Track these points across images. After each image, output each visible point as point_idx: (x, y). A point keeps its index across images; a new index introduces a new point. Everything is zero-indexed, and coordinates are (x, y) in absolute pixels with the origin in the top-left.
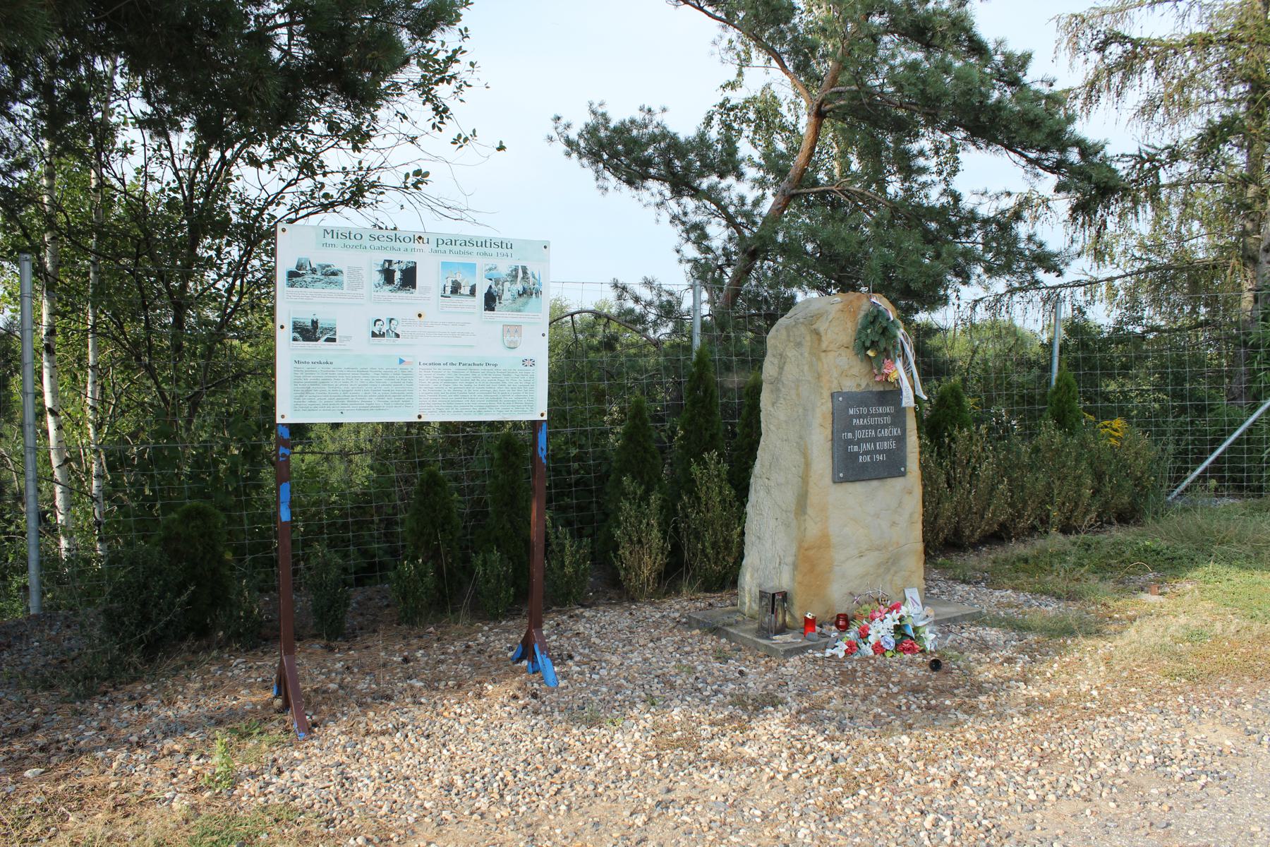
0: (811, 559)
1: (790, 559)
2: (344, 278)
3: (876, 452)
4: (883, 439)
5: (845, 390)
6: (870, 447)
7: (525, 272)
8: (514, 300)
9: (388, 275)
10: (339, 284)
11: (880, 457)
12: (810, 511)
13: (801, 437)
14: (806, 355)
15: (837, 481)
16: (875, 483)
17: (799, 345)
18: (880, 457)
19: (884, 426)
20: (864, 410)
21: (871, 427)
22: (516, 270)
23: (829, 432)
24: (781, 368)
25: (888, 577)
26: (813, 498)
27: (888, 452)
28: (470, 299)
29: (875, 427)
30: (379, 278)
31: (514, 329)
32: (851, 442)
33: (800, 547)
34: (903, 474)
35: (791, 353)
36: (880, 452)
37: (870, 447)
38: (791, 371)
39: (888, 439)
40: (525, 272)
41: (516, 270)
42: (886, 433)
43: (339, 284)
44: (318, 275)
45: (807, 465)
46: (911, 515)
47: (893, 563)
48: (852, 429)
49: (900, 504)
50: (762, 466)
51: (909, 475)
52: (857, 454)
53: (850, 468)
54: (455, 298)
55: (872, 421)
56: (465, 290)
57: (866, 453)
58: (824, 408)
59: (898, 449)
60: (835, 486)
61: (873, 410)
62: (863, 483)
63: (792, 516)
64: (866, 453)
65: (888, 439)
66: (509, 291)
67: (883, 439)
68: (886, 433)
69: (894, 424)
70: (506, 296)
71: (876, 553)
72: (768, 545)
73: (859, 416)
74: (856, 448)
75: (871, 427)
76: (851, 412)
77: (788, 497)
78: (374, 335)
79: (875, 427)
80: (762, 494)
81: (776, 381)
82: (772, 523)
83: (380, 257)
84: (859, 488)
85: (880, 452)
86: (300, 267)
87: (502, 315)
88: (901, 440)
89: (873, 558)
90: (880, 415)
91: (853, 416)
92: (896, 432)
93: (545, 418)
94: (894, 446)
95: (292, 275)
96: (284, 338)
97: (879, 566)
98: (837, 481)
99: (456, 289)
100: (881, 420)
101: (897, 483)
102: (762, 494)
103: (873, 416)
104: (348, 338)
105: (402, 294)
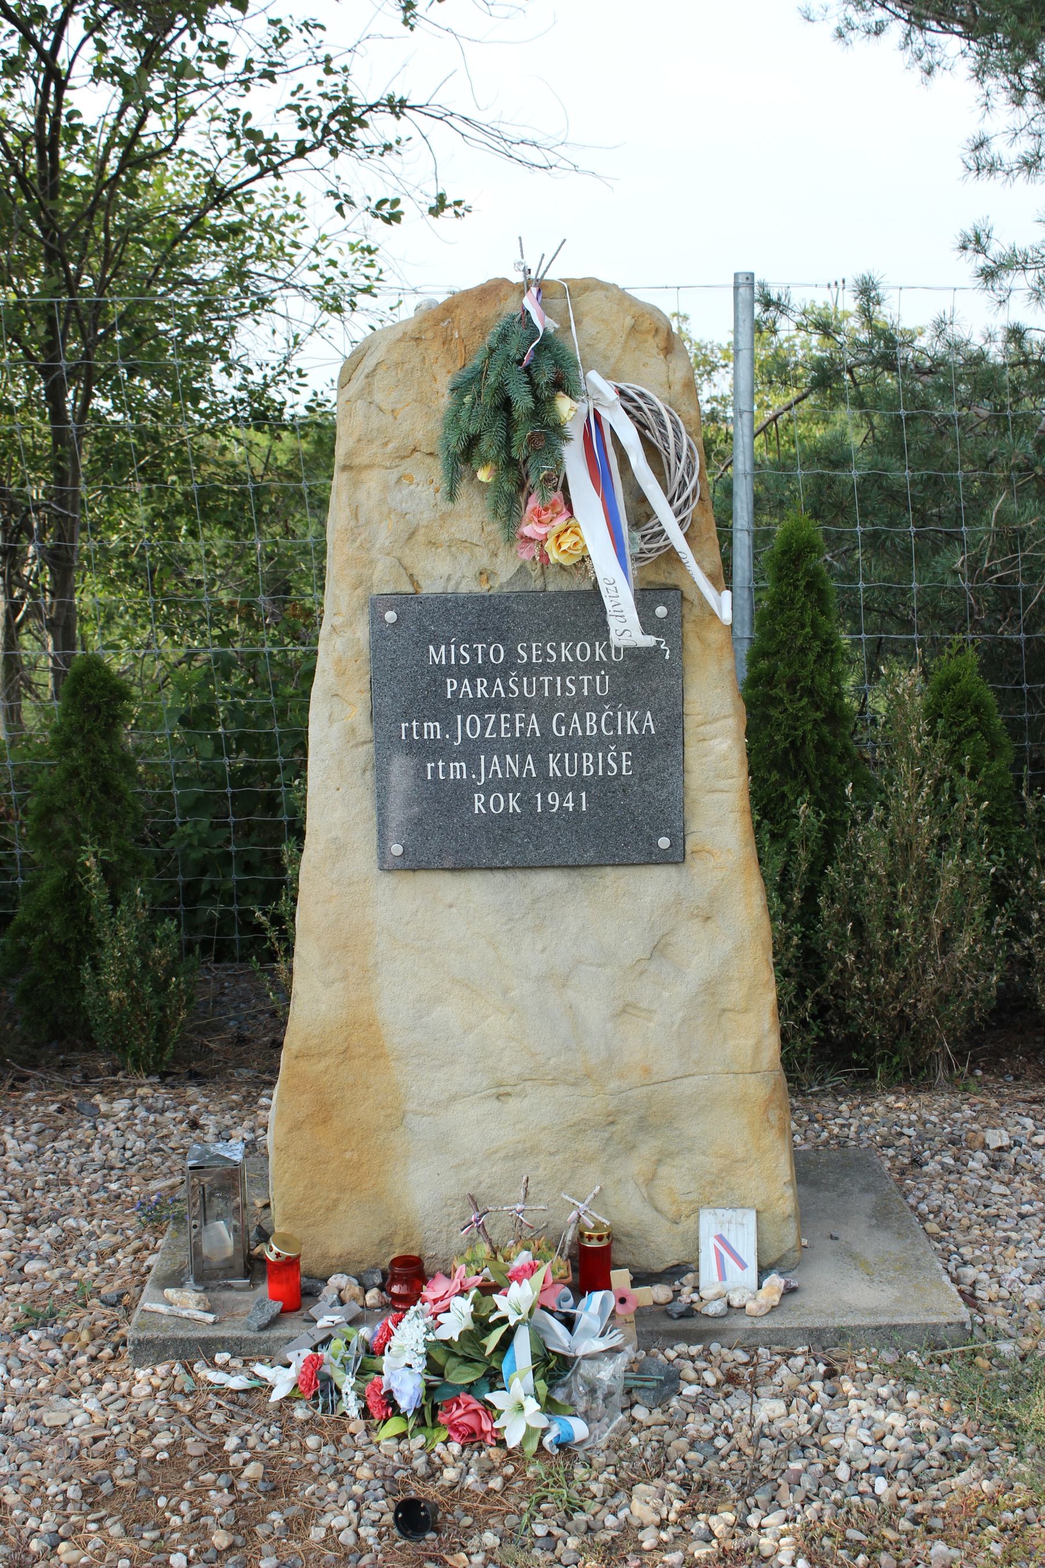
3: (546, 782)
4: (575, 745)
5: (430, 587)
16: (546, 881)
19: (581, 704)
25: (636, 1166)
27: (602, 788)
34: (676, 857)
36: (562, 785)
39: (599, 744)
42: (591, 724)
46: (710, 987)
47: (643, 1125)
48: (445, 711)
49: (659, 949)
51: (696, 866)
52: (463, 791)
55: (524, 688)
59: (644, 778)
60: (389, 881)
61: (528, 653)
62: (499, 877)
65: (599, 744)
68: (591, 724)
69: (624, 697)
71: (561, 1091)
73: (473, 672)
74: (458, 770)
76: (437, 655)
79: (545, 708)
85: (562, 785)
89: (538, 1110)
90: (562, 669)
91: (446, 671)
97: (579, 1128)
103: (529, 669)
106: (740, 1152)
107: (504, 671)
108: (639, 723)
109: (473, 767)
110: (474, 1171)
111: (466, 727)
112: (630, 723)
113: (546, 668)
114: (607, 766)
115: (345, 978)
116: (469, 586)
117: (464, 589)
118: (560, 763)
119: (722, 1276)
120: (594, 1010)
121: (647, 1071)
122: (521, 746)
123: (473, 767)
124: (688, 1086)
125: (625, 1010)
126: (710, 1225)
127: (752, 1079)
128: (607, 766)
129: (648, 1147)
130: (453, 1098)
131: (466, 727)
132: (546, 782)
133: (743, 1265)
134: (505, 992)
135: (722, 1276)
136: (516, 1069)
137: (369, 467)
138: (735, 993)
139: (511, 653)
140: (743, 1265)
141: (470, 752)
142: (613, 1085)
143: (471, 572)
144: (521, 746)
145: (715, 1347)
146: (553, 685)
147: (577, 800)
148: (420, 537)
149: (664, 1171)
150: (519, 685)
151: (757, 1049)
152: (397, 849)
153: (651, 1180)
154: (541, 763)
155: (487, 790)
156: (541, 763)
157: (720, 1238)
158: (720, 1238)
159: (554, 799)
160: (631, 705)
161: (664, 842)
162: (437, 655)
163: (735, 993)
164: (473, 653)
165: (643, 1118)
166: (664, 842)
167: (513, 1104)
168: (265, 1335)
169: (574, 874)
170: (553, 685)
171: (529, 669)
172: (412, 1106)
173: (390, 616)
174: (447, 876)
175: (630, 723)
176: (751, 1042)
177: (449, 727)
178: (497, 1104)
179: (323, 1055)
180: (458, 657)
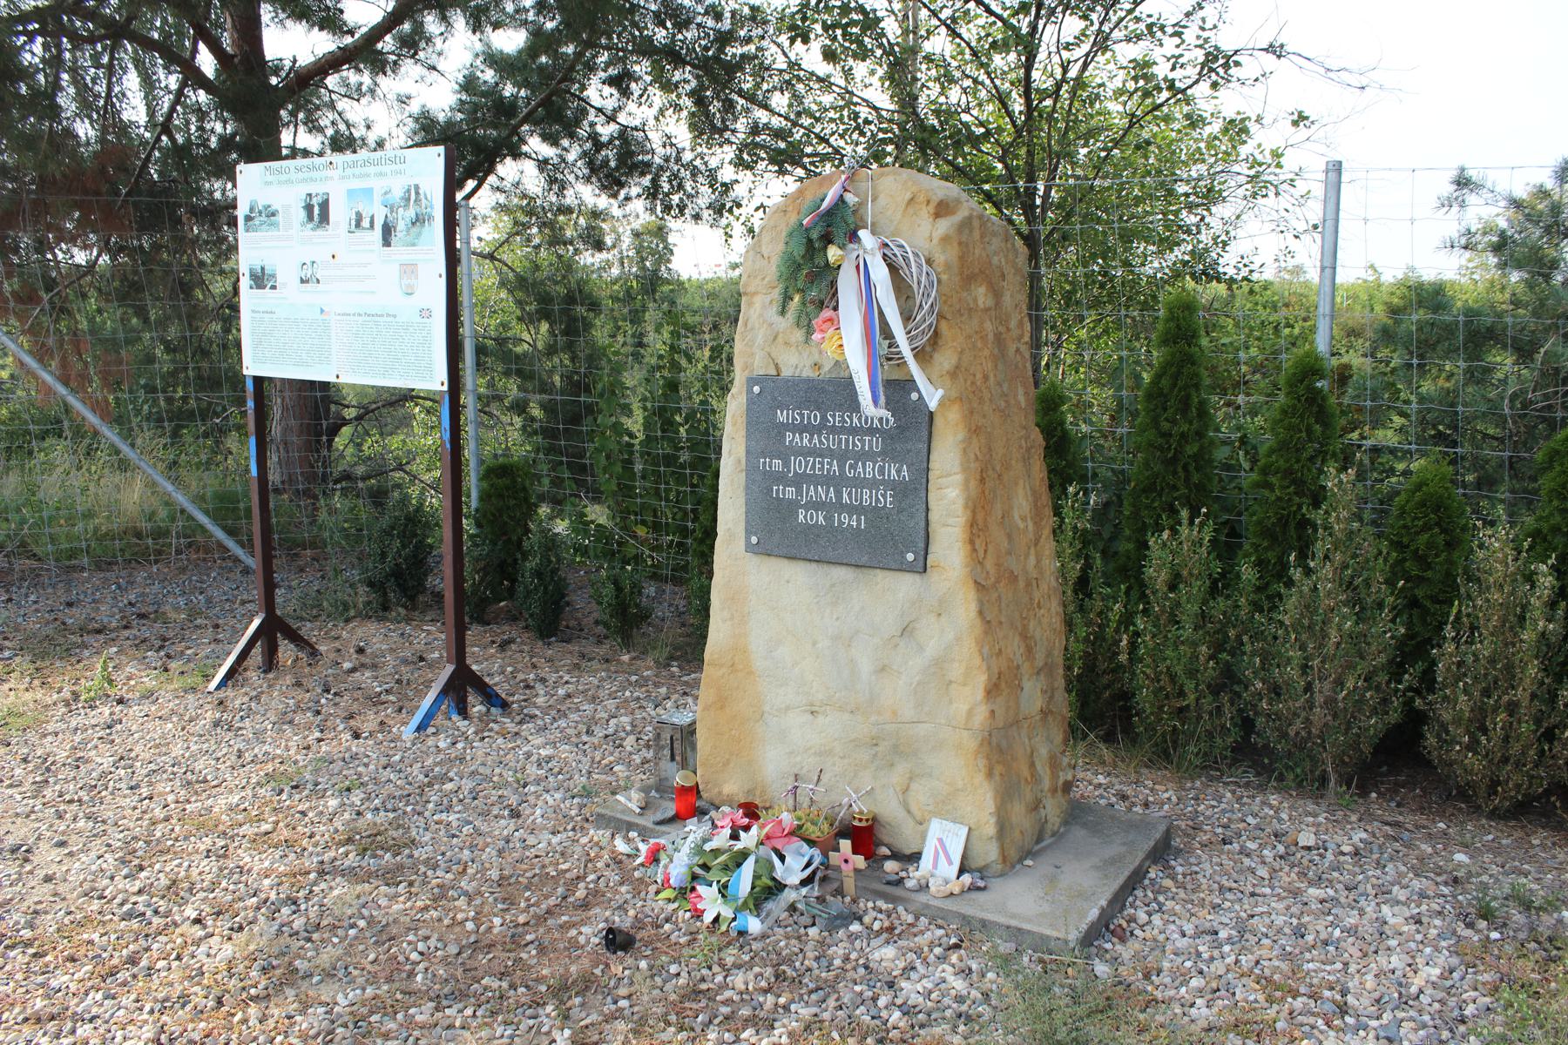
2: (279, 218)
3: (841, 507)
4: (859, 483)
5: (786, 372)
7: (417, 193)
8: (408, 230)
9: (309, 208)
10: (275, 225)
11: (849, 521)
19: (864, 456)
20: (815, 418)
21: (830, 453)
22: (409, 191)
25: (897, 776)
27: (874, 513)
28: (369, 233)
29: (842, 457)
30: (303, 214)
31: (409, 269)
32: (780, 478)
36: (851, 510)
39: (873, 484)
40: (417, 193)
41: (409, 191)
42: (869, 470)
43: (275, 225)
44: (263, 218)
46: (939, 664)
49: (906, 631)
51: (933, 575)
52: (793, 506)
54: (359, 234)
56: (366, 223)
57: (817, 506)
64: (817, 506)
65: (873, 484)
66: (404, 217)
67: (859, 483)
68: (869, 470)
70: (401, 226)
73: (802, 429)
75: (830, 453)
76: (782, 417)
78: (302, 281)
79: (842, 457)
83: (301, 191)
86: (252, 210)
87: (399, 252)
93: (445, 388)
94: (887, 500)
95: (248, 219)
96: (245, 283)
99: (358, 225)
100: (856, 443)
101: (904, 586)
103: (834, 430)
104: (284, 284)
105: (320, 232)
106: (960, 784)
107: (818, 430)
108: (899, 472)
109: (799, 492)
110: (798, 759)
111: (797, 465)
112: (893, 472)
113: (843, 430)
114: (878, 500)
115: (732, 619)
116: (808, 373)
117: (804, 375)
118: (850, 494)
119: (935, 866)
120: (866, 666)
121: (895, 713)
122: (826, 480)
123: (799, 492)
124: (922, 729)
125: (882, 669)
126: (936, 828)
127: (965, 733)
128: (878, 500)
129: (902, 769)
130: (788, 708)
132: (841, 507)
133: (950, 863)
134: (814, 644)
135: (935, 866)
136: (820, 696)
137: (755, 293)
138: (956, 671)
139: (824, 418)
140: (950, 863)
141: (799, 481)
142: (873, 718)
143: (809, 363)
144: (826, 480)
145: (900, 909)
146: (847, 441)
147: (859, 521)
148: (780, 339)
150: (827, 439)
151: (970, 713)
152: (754, 540)
153: (906, 790)
154: (839, 494)
155: (807, 507)
156: (839, 494)
157: (940, 840)
158: (940, 840)
159: (845, 518)
160: (894, 460)
161: (910, 557)
162: (782, 417)
163: (956, 671)
164: (802, 415)
165: (895, 746)
166: (910, 557)
167: (820, 719)
168: (658, 828)
169: (858, 570)
170: (847, 441)
171: (834, 430)
172: (767, 708)
173: (756, 389)
174: (786, 561)
175: (893, 472)
176: (966, 707)
177: (786, 464)
178: (810, 717)
179: (722, 666)
180: (794, 419)
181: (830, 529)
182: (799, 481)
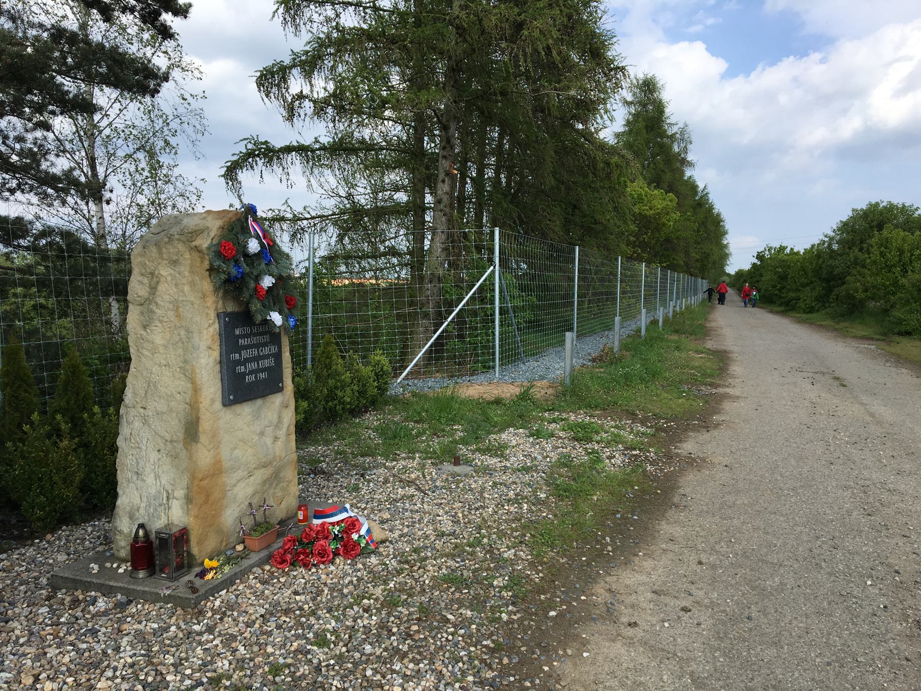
0: (203, 490)
1: (180, 493)
6: (253, 366)
11: (262, 376)
12: (203, 439)
13: (185, 362)
14: (187, 274)
15: (227, 403)
16: (259, 402)
17: (174, 263)
18: (262, 376)
23: (216, 354)
24: (153, 289)
25: (271, 491)
26: (205, 425)
29: (257, 346)
32: (239, 363)
33: (193, 477)
34: (281, 390)
35: (165, 272)
36: (262, 370)
37: (253, 366)
38: (166, 291)
45: (196, 390)
48: (239, 349)
50: (135, 394)
52: (244, 375)
53: (240, 389)
57: (251, 372)
58: (211, 329)
62: (250, 402)
63: (181, 446)
64: (251, 372)
68: (266, 351)
72: (150, 479)
76: (237, 332)
77: (174, 426)
80: (137, 424)
81: (147, 302)
82: (153, 456)
84: (246, 410)
85: (262, 370)
88: (278, 357)
89: (260, 475)
92: (274, 349)
97: (264, 482)
98: (227, 403)
101: (277, 400)
102: (137, 424)
111: (245, 354)
131: (245, 354)
149: (276, 491)
167: (252, 478)
177: (240, 356)
181: (257, 382)
182: (244, 363)
